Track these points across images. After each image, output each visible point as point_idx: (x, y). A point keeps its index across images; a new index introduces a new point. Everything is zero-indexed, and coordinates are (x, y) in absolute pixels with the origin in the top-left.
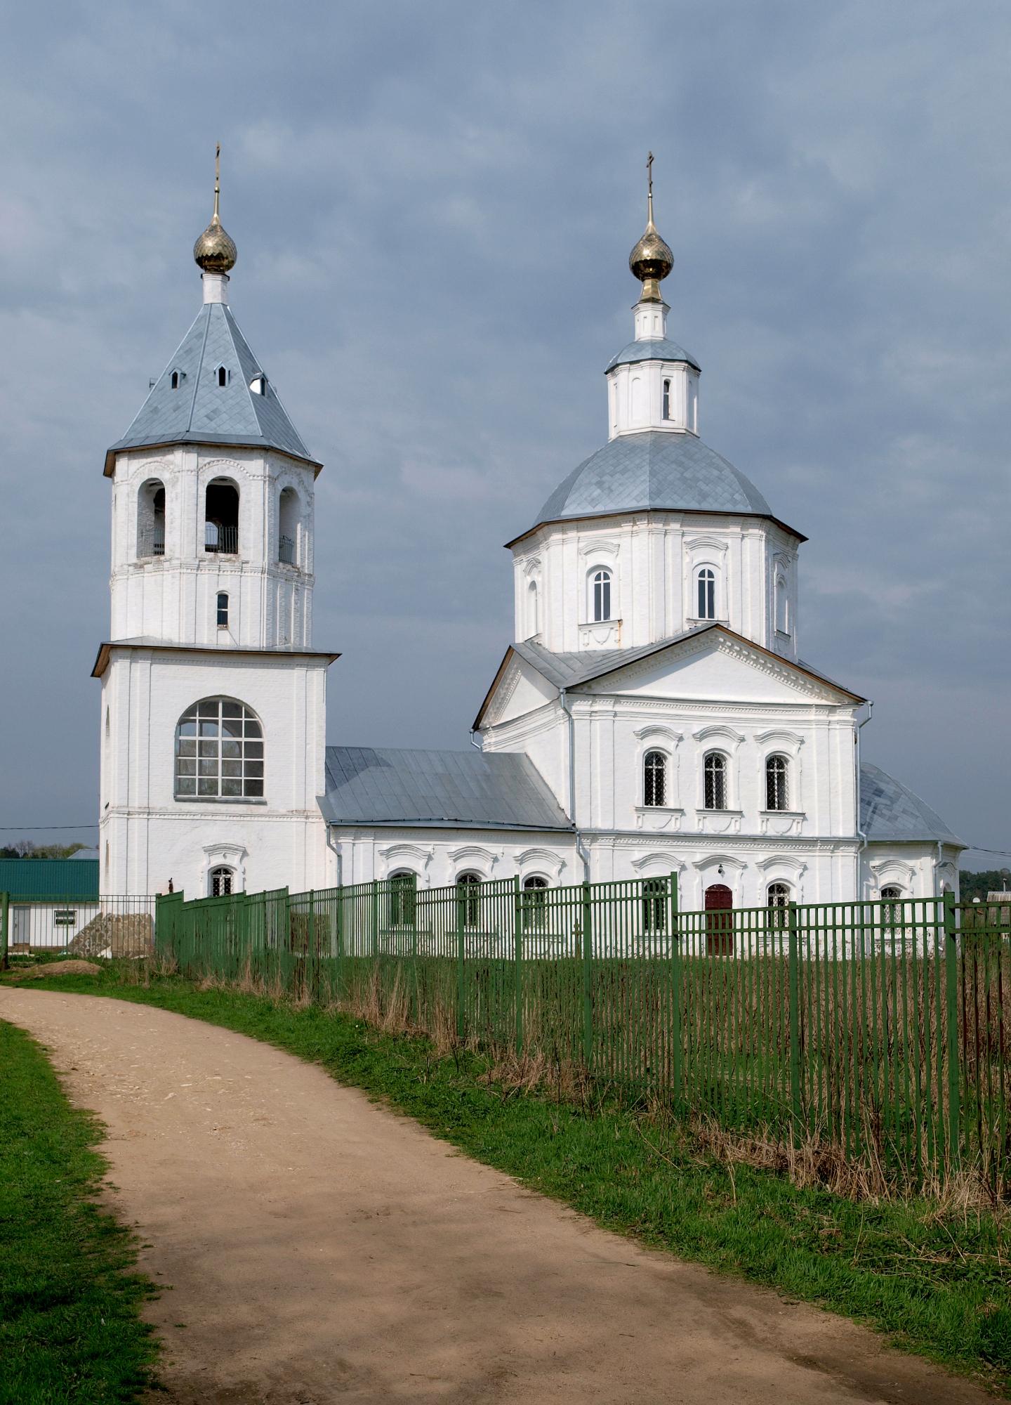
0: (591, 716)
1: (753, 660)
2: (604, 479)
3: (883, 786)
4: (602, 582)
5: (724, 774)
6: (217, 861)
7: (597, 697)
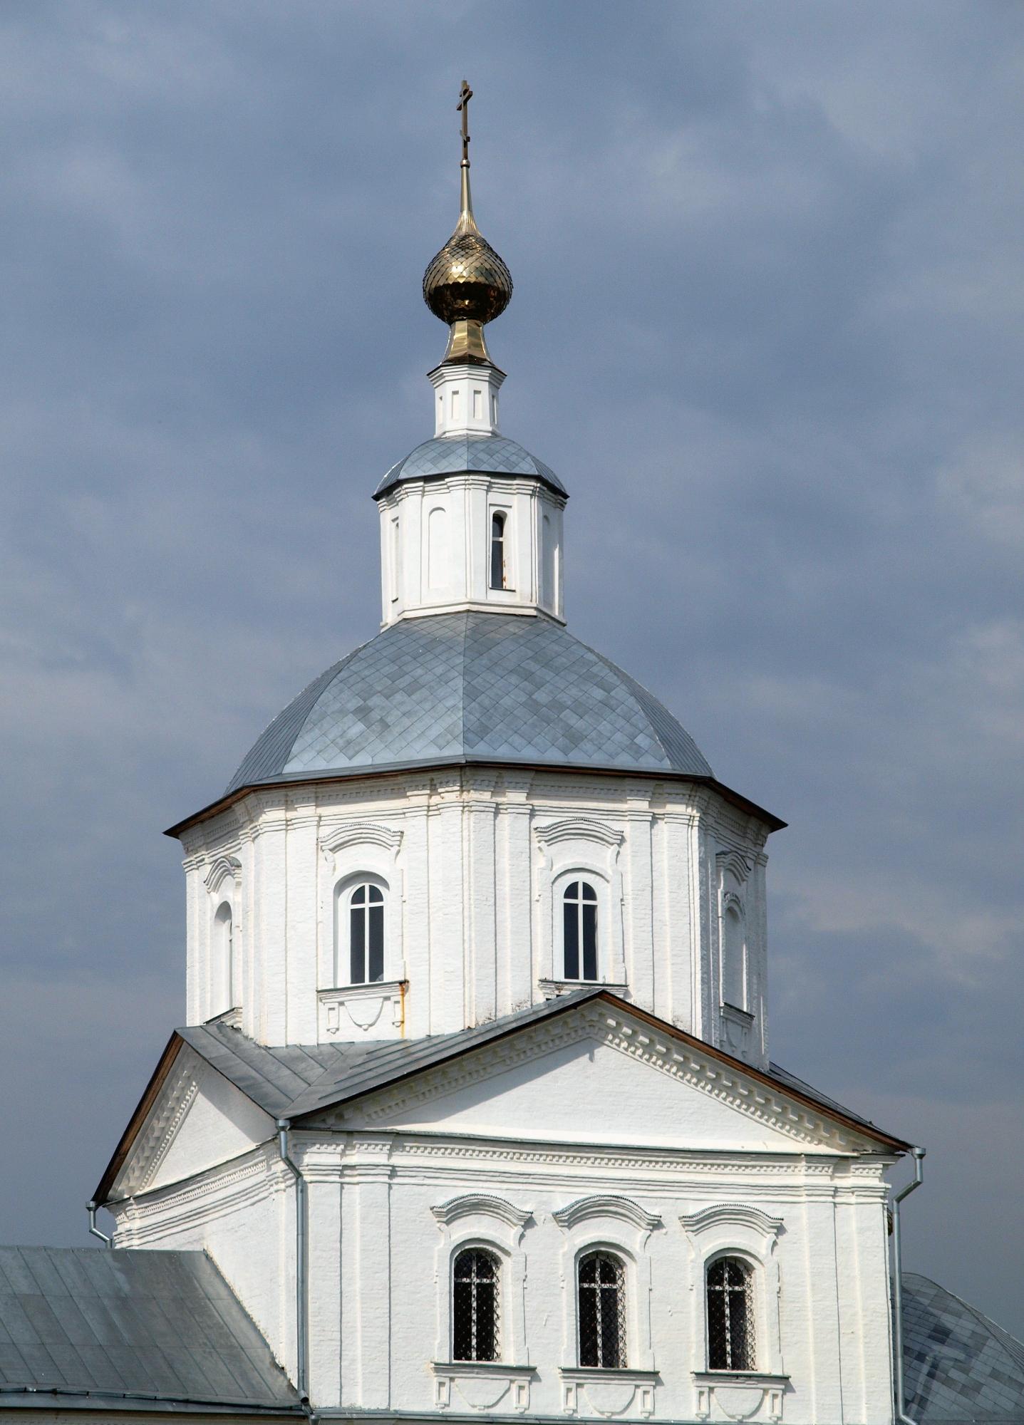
0: (341, 1176)
1: (676, 1062)
2: (370, 703)
3: (948, 1321)
4: (367, 905)
5: (620, 1295)
7: (356, 1135)
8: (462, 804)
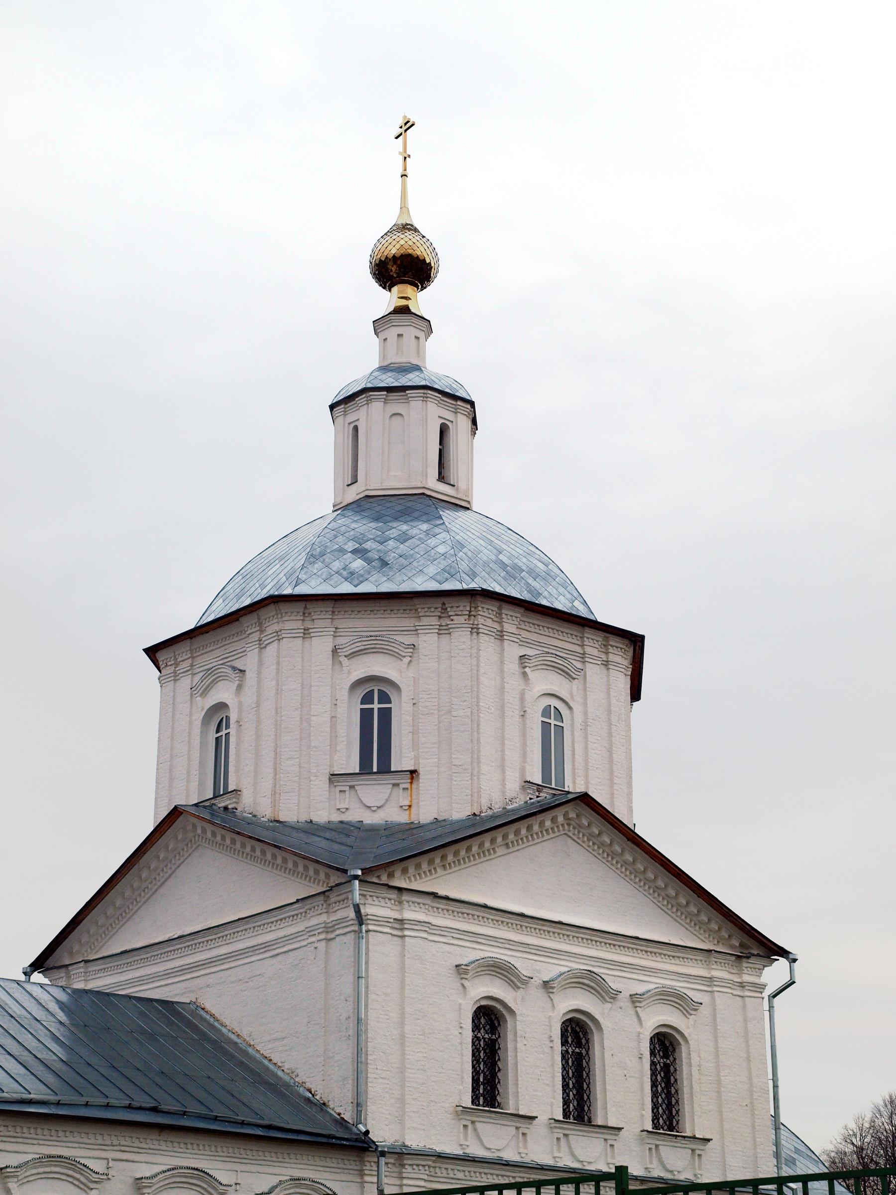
8: (471, 626)
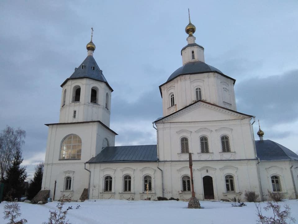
4: (172, 97)
6: (67, 175)
